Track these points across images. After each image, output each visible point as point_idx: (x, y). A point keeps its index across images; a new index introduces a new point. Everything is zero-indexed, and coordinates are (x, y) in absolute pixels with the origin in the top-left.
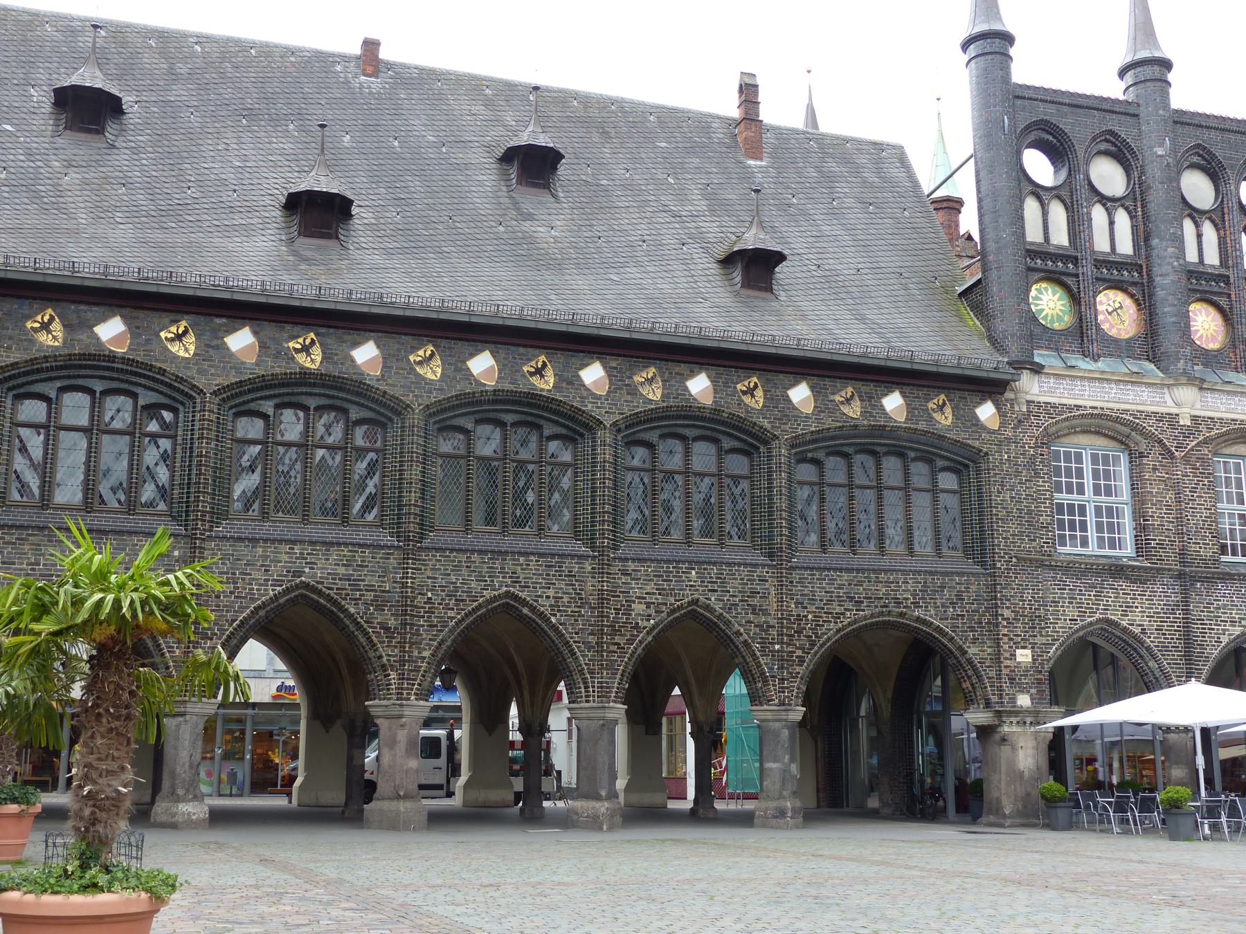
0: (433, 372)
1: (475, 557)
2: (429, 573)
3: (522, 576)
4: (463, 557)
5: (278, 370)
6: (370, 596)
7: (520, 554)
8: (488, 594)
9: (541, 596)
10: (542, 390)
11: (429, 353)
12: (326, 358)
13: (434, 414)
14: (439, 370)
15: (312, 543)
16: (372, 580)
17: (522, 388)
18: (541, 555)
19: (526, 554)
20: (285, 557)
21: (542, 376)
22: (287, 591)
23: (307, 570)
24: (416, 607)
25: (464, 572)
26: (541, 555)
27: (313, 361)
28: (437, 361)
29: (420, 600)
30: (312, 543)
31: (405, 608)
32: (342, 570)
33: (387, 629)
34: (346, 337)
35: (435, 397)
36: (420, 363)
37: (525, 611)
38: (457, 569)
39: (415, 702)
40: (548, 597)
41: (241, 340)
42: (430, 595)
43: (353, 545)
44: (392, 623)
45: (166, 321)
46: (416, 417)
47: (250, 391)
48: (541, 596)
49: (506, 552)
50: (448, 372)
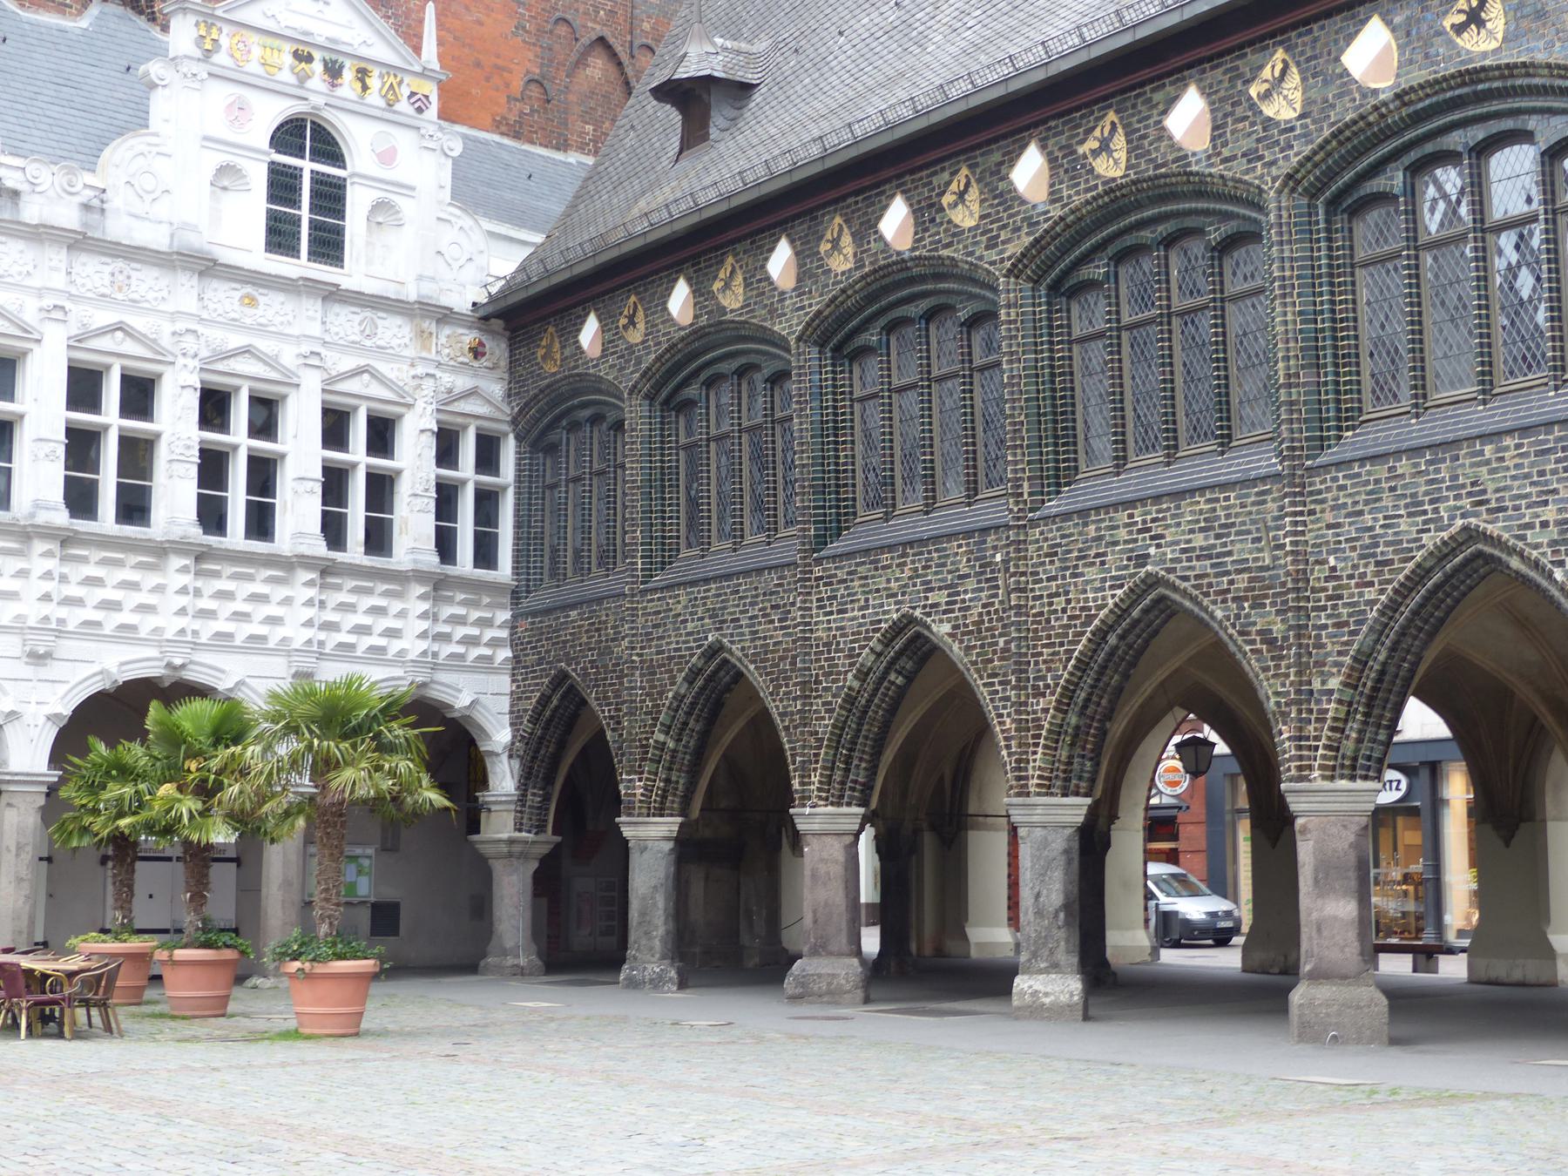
0: (1283, 108)
1: (1403, 466)
2: (1329, 517)
3: (1491, 487)
4: (1381, 471)
5: (1077, 200)
6: (1242, 581)
7: (1485, 437)
8: (1431, 540)
9: (1530, 526)
10: (1485, 55)
11: (1279, 66)
12: (1134, 148)
13: (1320, 191)
14: (1298, 95)
15: (1157, 499)
16: (1242, 549)
17: (1447, 69)
18: (1525, 430)
19: (1499, 434)
20: (1122, 534)
21: (1481, 24)
22: (1135, 595)
23: (1152, 551)
24: (1314, 590)
25: (1387, 501)
26: (1525, 430)
27: (1112, 167)
28: (1294, 78)
29: (1319, 572)
30: (1157, 499)
31: (1297, 593)
32: (1199, 540)
33: (1271, 642)
34: (1158, 97)
35: (1302, 149)
36: (1266, 96)
37: (1515, 563)
38: (1374, 497)
39: (1327, 785)
40: (1544, 524)
41: (1029, 171)
42: (1332, 562)
43: (1212, 487)
44: (1278, 628)
45: (946, 176)
46: (1278, 207)
47: (1064, 251)
48: (1530, 526)
49: (1456, 443)
50: (1313, 94)
